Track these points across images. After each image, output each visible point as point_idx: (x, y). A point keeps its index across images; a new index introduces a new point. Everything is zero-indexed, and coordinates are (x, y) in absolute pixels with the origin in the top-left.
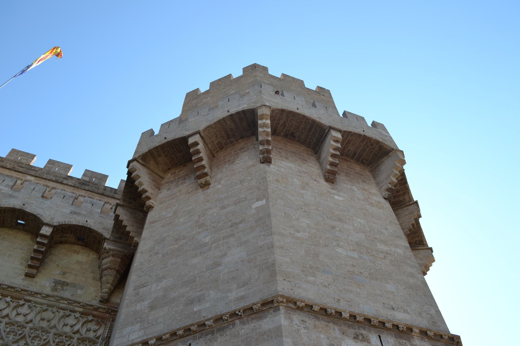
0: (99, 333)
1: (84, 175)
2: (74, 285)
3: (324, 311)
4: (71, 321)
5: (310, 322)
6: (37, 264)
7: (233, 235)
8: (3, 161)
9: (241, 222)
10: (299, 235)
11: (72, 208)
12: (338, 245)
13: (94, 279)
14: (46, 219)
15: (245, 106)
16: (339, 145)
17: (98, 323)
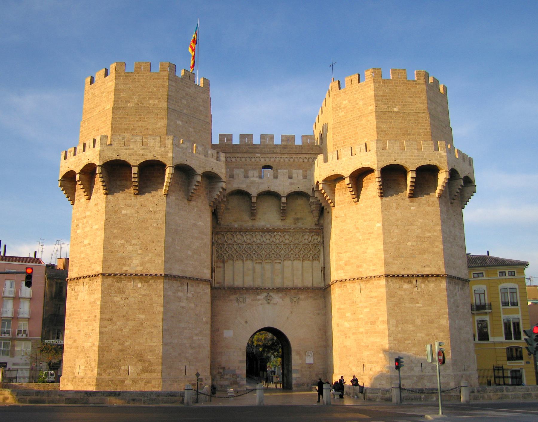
0: (319, 239)
1: (282, 140)
2: (302, 219)
3: (398, 276)
4: (306, 237)
5: (394, 280)
6: (284, 213)
7: (369, 239)
8: (240, 147)
9: (372, 233)
10: (393, 241)
11: (290, 180)
12: (409, 241)
13: (309, 212)
14: (281, 193)
15: (369, 163)
16: (414, 180)
17: (317, 235)
